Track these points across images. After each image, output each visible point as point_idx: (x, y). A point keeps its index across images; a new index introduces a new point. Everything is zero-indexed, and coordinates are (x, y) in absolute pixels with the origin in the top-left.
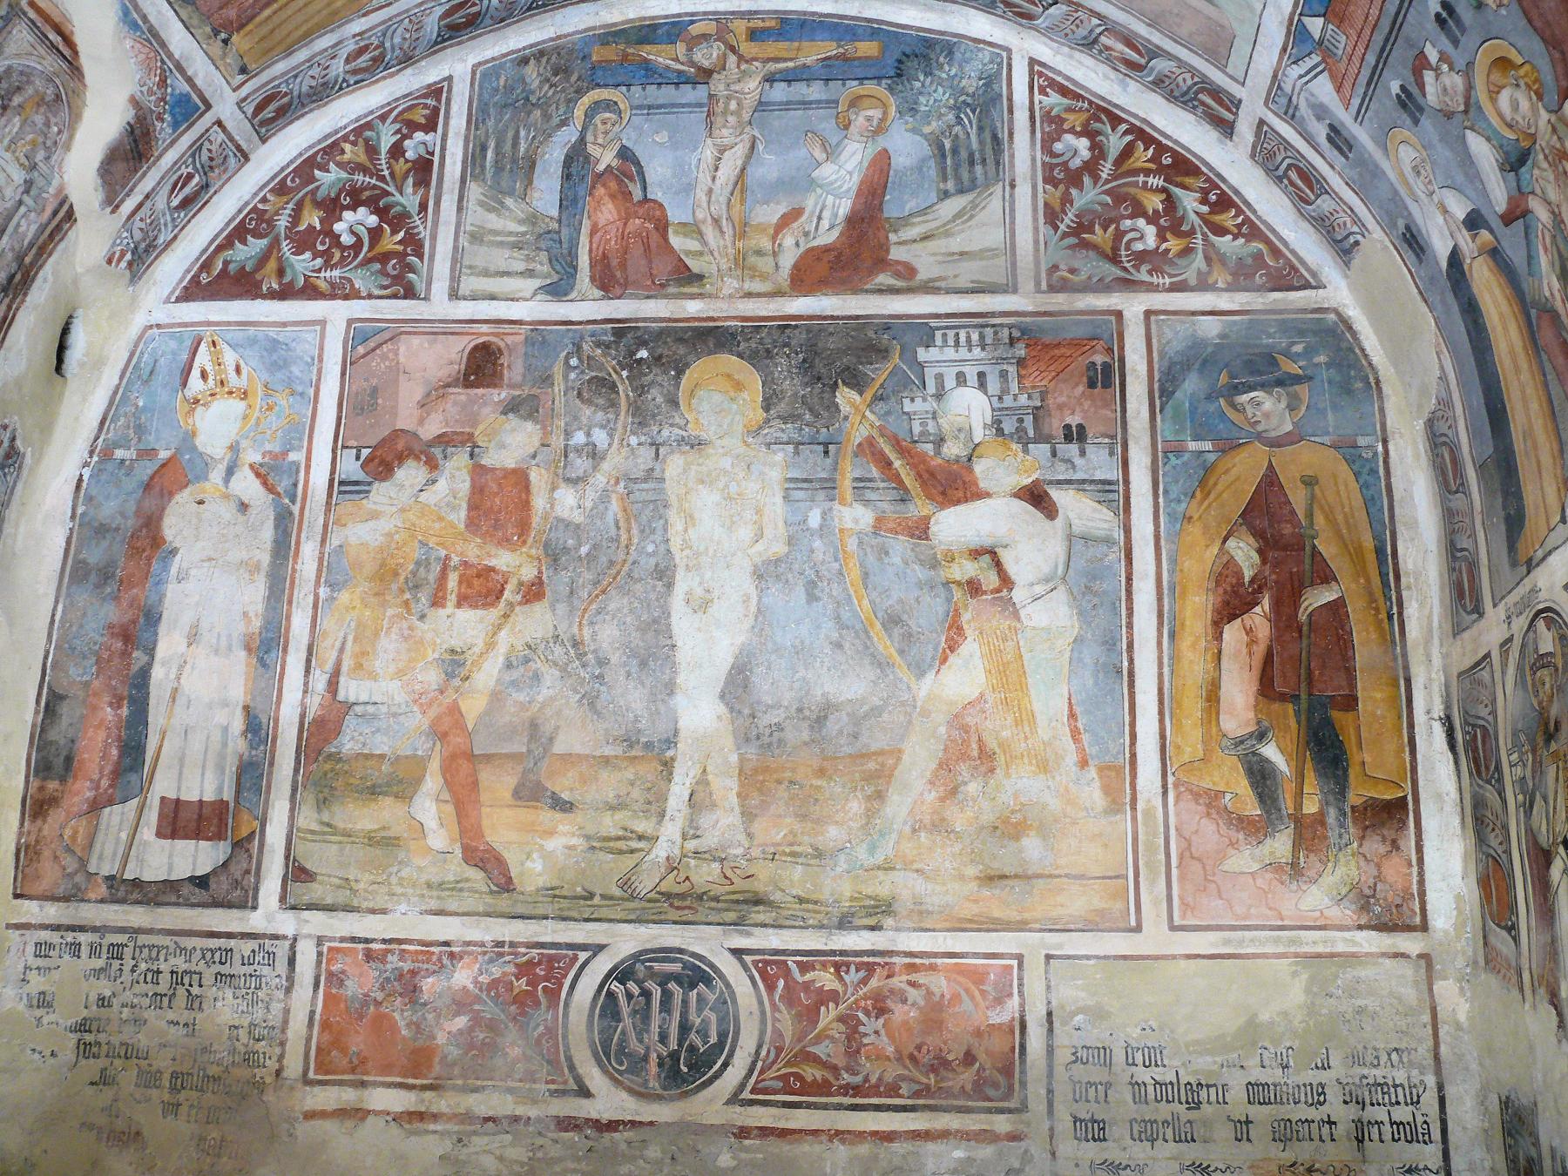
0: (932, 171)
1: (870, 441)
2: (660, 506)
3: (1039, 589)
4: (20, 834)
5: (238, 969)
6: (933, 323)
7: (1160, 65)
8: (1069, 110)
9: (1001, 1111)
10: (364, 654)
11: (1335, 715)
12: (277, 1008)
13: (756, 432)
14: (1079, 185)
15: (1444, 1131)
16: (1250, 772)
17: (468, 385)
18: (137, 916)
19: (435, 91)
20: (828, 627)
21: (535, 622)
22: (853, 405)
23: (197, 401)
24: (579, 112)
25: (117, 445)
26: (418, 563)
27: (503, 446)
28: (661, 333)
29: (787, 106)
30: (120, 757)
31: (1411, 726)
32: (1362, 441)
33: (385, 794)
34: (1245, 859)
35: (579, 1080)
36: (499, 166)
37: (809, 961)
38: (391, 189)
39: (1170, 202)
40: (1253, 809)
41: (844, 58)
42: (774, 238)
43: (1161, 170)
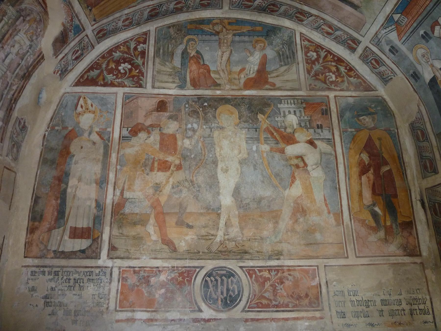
0: (278, 60)
1: (267, 128)
2: (213, 145)
3: (314, 167)
4: (26, 239)
5: (95, 277)
6: (281, 98)
7: (338, 33)
8: (311, 46)
9: (317, 311)
10: (131, 184)
11: (392, 199)
12: (107, 288)
13: (237, 125)
14: (315, 64)
15: (433, 311)
16: (372, 214)
17: (158, 111)
18: (63, 262)
19: (146, 34)
20: (260, 176)
21: (180, 176)
22: (262, 118)
23: (80, 114)
24: (185, 41)
25: (56, 126)
26: (146, 159)
27: (168, 128)
28: (210, 99)
29: (239, 42)
30: (58, 214)
31: (412, 202)
32: (392, 129)
33: (138, 224)
34: (373, 238)
35: (199, 307)
36: (165, 55)
37: (261, 269)
38: (134, 59)
39: (338, 69)
40: (374, 225)
41: (253, 30)
42: (239, 75)
43: (334, 61)
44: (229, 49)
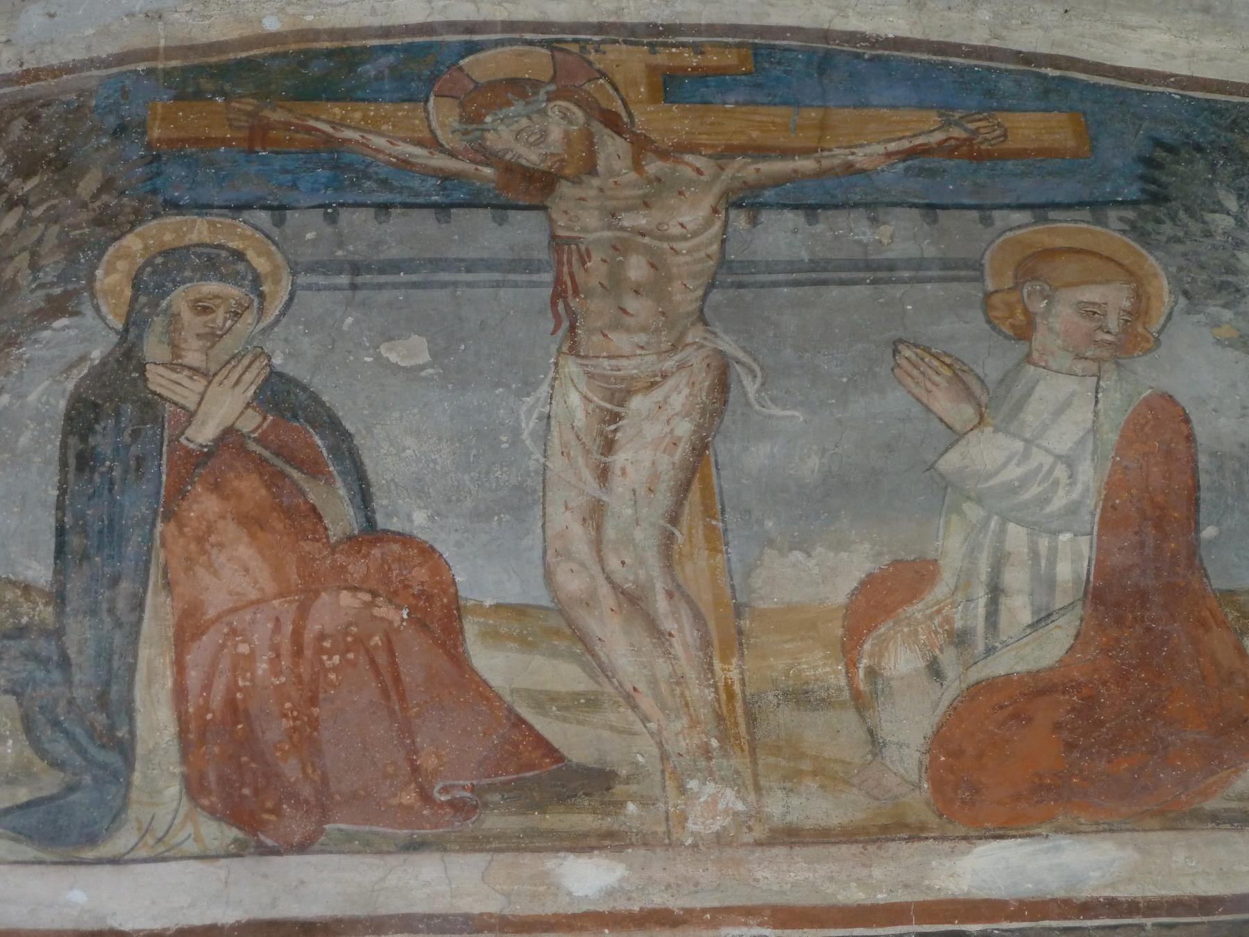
24: (113, 277)
29: (817, 273)
42: (849, 650)
44: (697, 359)
